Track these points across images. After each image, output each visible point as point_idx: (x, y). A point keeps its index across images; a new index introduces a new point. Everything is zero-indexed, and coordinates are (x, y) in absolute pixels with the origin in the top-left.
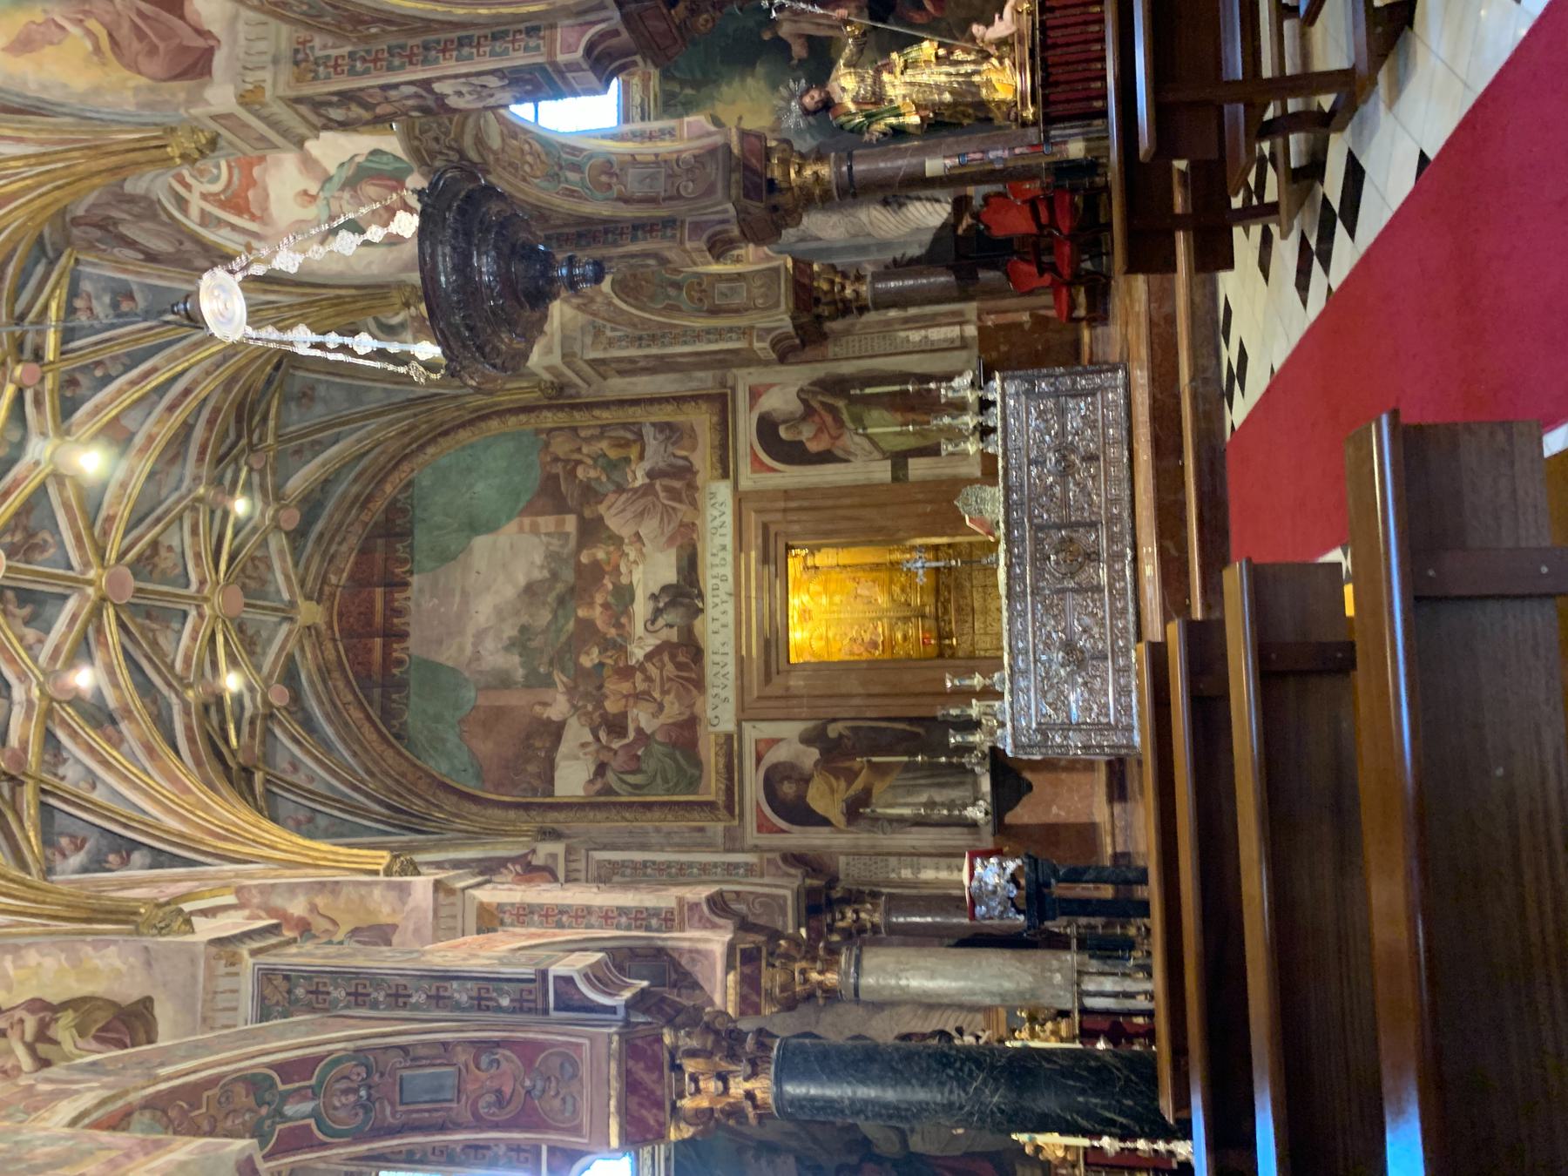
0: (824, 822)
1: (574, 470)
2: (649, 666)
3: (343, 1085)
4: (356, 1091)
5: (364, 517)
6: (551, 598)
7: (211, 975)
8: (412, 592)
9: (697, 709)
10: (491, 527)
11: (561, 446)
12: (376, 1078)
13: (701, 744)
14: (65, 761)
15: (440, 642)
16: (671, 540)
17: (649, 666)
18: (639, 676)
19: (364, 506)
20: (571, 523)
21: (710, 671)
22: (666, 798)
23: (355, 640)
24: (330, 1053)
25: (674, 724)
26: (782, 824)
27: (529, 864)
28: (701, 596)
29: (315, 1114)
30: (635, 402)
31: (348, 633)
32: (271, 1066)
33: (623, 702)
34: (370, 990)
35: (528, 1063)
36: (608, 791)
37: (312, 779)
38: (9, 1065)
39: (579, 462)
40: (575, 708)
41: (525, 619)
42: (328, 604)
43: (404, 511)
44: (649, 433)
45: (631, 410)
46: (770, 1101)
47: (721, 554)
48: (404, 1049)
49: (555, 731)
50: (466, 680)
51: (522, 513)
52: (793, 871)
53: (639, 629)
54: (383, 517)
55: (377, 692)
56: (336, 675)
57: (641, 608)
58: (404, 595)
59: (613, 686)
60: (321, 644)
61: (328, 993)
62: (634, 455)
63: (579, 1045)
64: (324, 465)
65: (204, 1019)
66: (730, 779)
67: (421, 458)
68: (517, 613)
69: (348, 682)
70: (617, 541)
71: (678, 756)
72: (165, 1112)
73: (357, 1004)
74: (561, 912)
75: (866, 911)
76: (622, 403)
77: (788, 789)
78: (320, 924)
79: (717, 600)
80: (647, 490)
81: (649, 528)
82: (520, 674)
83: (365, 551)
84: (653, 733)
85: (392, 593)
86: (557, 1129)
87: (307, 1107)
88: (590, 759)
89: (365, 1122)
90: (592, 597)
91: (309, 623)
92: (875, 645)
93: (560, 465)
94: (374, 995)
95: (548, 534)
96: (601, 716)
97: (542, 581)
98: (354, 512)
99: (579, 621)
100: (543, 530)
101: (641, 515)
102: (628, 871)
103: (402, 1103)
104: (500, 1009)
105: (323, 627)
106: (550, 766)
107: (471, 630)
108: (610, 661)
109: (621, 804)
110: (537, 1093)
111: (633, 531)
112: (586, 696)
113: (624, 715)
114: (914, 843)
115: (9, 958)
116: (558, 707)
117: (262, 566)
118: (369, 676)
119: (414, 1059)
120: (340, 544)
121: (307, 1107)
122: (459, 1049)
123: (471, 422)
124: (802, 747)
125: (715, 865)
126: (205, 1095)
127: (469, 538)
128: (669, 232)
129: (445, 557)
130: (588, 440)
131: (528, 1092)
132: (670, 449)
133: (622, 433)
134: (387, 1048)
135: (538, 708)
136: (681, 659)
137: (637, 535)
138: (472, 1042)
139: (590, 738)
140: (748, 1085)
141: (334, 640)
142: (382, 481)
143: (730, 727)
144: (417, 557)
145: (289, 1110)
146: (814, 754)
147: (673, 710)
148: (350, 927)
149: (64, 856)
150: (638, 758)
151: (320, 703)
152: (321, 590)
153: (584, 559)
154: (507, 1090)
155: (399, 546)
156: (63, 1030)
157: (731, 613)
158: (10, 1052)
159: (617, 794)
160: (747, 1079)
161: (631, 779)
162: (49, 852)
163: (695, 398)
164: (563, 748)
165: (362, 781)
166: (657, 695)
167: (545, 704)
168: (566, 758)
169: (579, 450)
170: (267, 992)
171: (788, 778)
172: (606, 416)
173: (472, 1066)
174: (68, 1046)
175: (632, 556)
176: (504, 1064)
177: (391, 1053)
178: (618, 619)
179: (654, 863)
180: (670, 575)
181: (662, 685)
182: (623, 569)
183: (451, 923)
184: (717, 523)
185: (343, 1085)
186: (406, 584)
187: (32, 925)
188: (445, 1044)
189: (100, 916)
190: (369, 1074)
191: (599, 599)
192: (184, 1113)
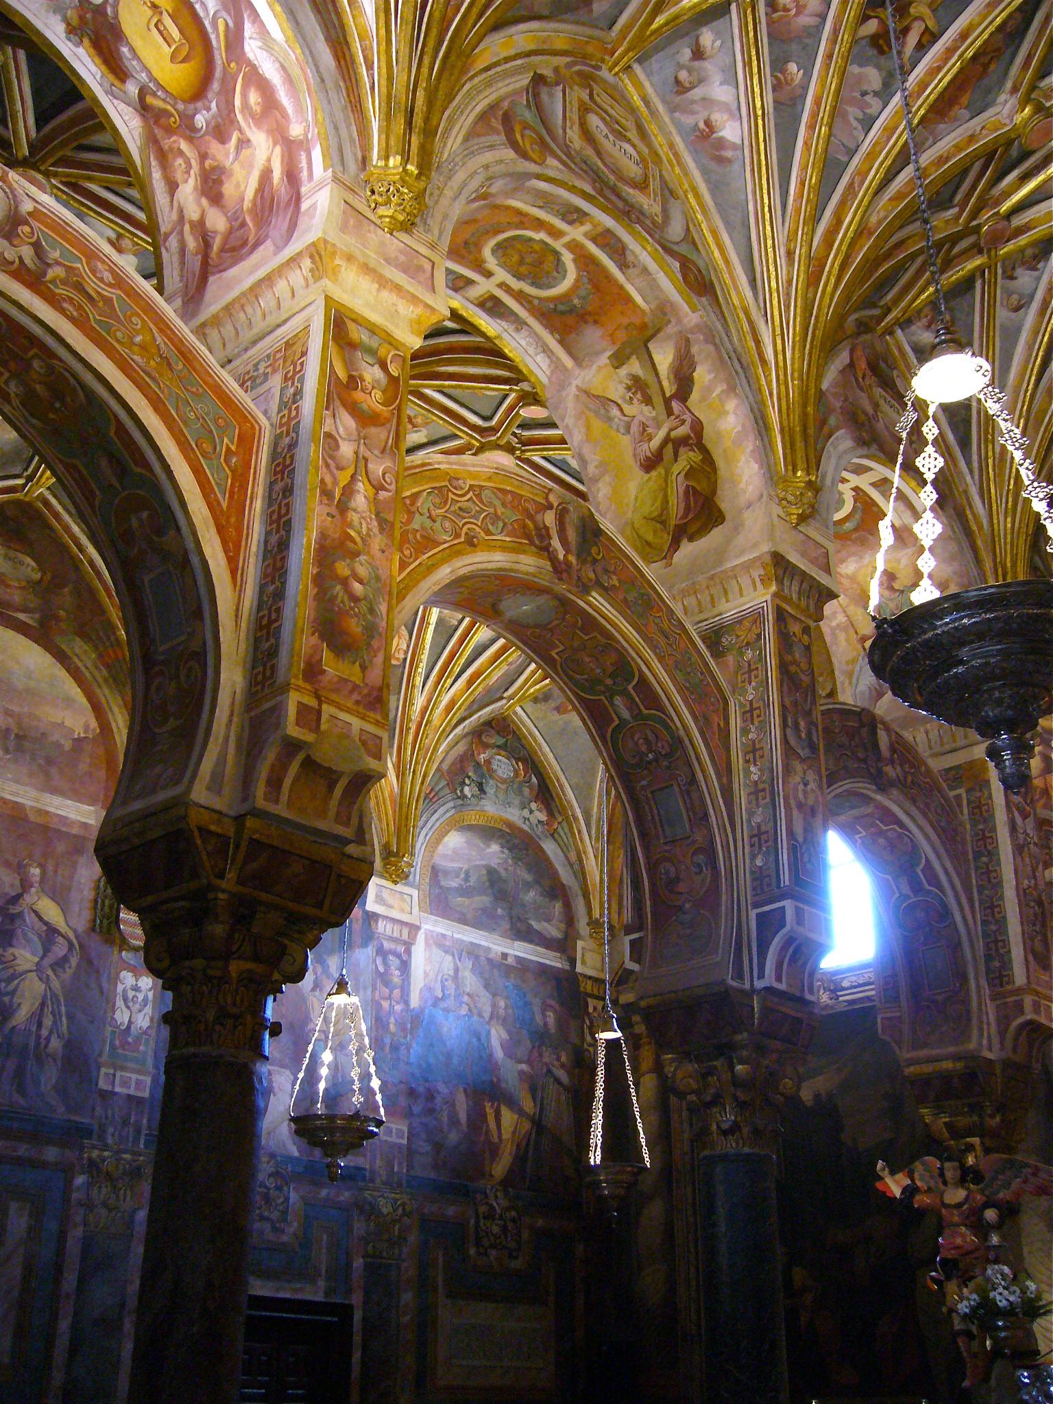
3: (651, 737)
4: (651, 751)
7: (747, 567)
12: (665, 763)
14: (1034, 269)
32: (640, 671)
34: (756, 722)
38: (650, 430)
48: (693, 781)
72: (566, 613)
73: (744, 713)
87: (626, 714)
104: (753, 857)
115: (725, 387)
119: (688, 792)
121: (626, 714)
126: (596, 634)
134: (690, 765)
138: (712, 842)
145: (618, 700)
149: (928, 327)
154: (682, 887)
156: (689, 457)
158: (659, 427)
162: (926, 310)
170: (746, 623)
173: (697, 846)
174: (676, 469)
176: (698, 879)
185: (651, 737)
187: (769, 384)
188: (706, 816)
189: (787, 438)
190: (669, 755)
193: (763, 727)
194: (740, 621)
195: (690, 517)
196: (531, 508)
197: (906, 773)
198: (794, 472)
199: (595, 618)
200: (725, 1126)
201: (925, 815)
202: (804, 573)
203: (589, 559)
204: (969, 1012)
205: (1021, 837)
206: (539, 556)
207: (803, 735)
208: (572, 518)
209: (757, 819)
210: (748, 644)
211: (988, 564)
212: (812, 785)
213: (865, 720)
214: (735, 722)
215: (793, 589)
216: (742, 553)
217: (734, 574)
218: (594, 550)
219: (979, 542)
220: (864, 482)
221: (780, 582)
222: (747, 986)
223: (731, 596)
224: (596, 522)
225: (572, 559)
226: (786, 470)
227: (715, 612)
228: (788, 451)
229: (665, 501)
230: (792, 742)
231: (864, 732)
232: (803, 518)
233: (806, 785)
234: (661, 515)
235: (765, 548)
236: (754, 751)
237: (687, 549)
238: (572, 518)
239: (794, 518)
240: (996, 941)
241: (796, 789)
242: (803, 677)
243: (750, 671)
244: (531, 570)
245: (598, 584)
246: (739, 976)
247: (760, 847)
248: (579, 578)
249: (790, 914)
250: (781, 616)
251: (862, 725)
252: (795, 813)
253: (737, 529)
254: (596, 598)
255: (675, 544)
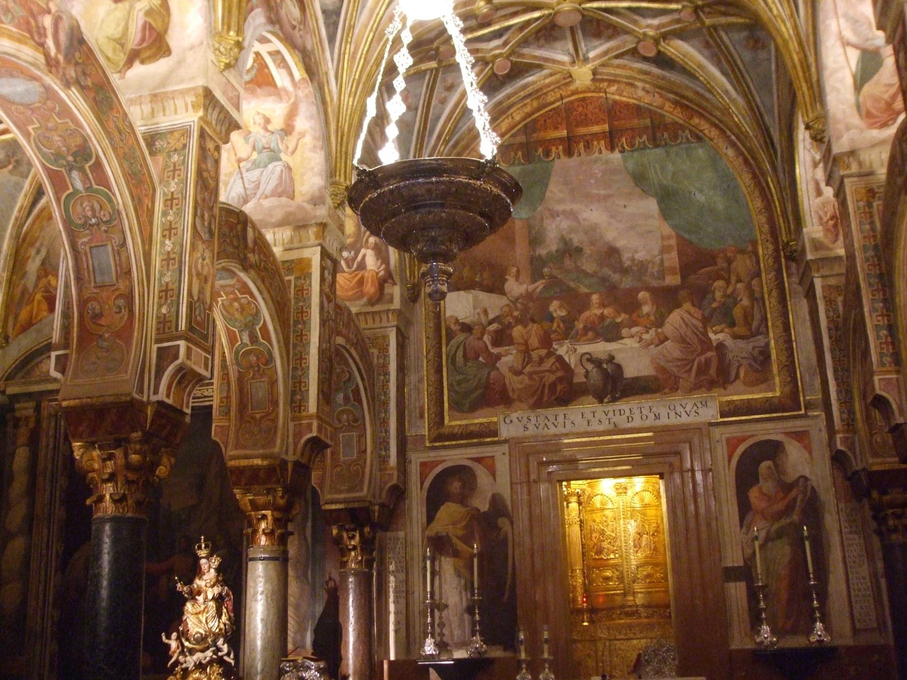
0: (430, 518)
1: (719, 277)
2: (552, 360)
5: (668, 106)
6: (607, 271)
7: (183, 93)
8: (607, 155)
9: (517, 404)
10: (665, 213)
11: (742, 264)
12: (104, 228)
13: (486, 410)
15: (565, 183)
16: (661, 369)
17: (552, 360)
18: (543, 352)
19: (676, 103)
20: (672, 280)
21: (550, 412)
22: (445, 384)
23: (564, 115)
24: (114, 194)
25: (505, 385)
26: (427, 484)
27: (385, 281)
28: (614, 400)
29: (76, 191)
30: (786, 327)
31: (570, 108)
32: (98, 157)
33: (521, 341)
34: (174, 208)
35: (118, 335)
36: (450, 335)
37: (443, 102)
39: (728, 282)
40: (517, 299)
41: (588, 251)
42: (593, 88)
43: (675, 137)
44: (760, 340)
45: (779, 323)
46: (100, 514)
47: (652, 416)
48: (124, 244)
49: (496, 287)
50: (535, 210)
51: (679, 237)
52: (384, 496)
53: (583, 348)
54: (668, 120)
55: (521, 139)
56: (535, 104)
57: (601, 348)
58: (603, 148)
59: (534, 328)
60: (559, 88)
61: (173, 179)
62: (736, 328)
63: (126, 372)
64: (700, 66)
65: (155, 95)
66: (462, 437)
67: (722, 144)
68: (592, 243)
69: (529, 115)
70: (659, 322)
71: (480, 391)
72: (48, 99)
73: (166, 200)
74: (304, 322)
75: (356, 556)
76: (785, 315)
77: (455, 486)
78: (291, 141)
79: (611, 415)
80: (706, 344)
81: (672, 349)
82: (542, 252)
83: (638, 110)
84: (498, 369)
85: (604, 138)
86: (77, 360)
87: (79, 185)
88: (475, 318)
89: (77, 225)
90: (609, 305)
91: (574, 76)
92: (600, 551)
93: (725, 265)
94: (171, 212)
95: (662, 261)
96: (510, 323)
97: (621, 262)
98: (672, 96)
99: (588, 296)
100: (666, 256)
101: (682, 340)
102: (381, 361)
103: (91, 248)
104: (160, 306)
105: (572, 87)
106: (468, 286)
107: (575, 207)
108: (555, 325)
109: (440, 348)
110: (100, 342)
111: (669, 335)
112: (526, 309)
113: (511, 342)
114: (416, 594)
116: (515, 287)
117: (610, 31)
118: (535, 132)
119: (119, 253)
120: (644, 89)
122: (128, 283)
123: (758, 184)
124: (489, 495)
125: (387, 431)
126: (68, 120)
127: (655, 195)
128: (887, 359)
129: (640, 179)
130: (749, 287)
131: (101, 336)
132: (744, 362)
133: (757, 316)
134: (123, 232)
135: (514, 270)
136: (559, 387)
137: (667, 339)
139: (491, 316)
140: (108, 497)
141: (562, 98)
142: (701, 116)
143: (505, 432)
144: (636, 154)
145: (75, 174)
146: (484, 507)
147: (515, 383)
148: (291, 165)
150: (477, 358)
151: (509, 97)
152: (602, 80)
153: (642, 295)
154: (103, 321)
155: (645, 137)
157: (601, 428)
159: (447, 345)
160: (111, 495)
161: (460, 354)
163: (794, 379)
164: (483, 296)
165: (446, 142)
166: (528, 369)
167: (517, 276)
168: (475, 299)
169: (739, 280)
170: (176, 135)
171: (463, 487)
172: (771, 303)
173: (117, 293)
175: (646, 337)
176: (118, 316)
177: (121, 236)
178: (591, 329)
179: (388, 381)
180: (631, 370)
181: (535, 373)
182: (635, 330)
183: (296, 240)
184: (679, 409)
186: (612, 149)
188: (129, 272)
191: (607, 311)
192: (53, 110)
193: (179, 214)
194: (171, 132)
195: (144, 45)
196: (35, 9)
197: (261, 260)
198: (228, 32)
199: (70, 108)
200: (116, 497)
201: (269, 292)
202: (222, 108)
203: (73, 61)
204: (276, 427)
205: (326, 314)
206: (36, 50)
207: (206, 224)
208: (64, 26)
209: (167, 279)
210: (176, 150)
211: (333, 127)
212: (207, 261)
213: (242, 219)
214: (159, 206)
215: (214, 116)
216: (182, 82)
217: (173, 95)
218: (77, 55)
219: (330, 110)
220: (263, 49)
221: (206, 109)
222: (145, 399)
223: (167, 112)
224: (81, 33)
225: (61, 58)
226: (223, 29)
227: (154, 121)
228: (226, 15)
229: (126, 28)
230: (199, 228)
231: (239, 227)
232: (228, 66)
233: (204, 260)
234: (120, 39)
235: (200, 82)
236: (170, 229)
237: (138, 69)
238: (64, 26)
239: (222, 66)
240: (300, 382)
241: (197, 262)
242: (211, 181)
243: (174, 170)
244: (30, 59)
245: (77, 82)
246: (141, 391)
247: (166, 299)
248: (64, 75)
249: (182, 351)
250: (202, 134)
251: (239, 223)
252: (195, 279)
253: (180, 63)
254: (74, 91)
255: (130, 63)
